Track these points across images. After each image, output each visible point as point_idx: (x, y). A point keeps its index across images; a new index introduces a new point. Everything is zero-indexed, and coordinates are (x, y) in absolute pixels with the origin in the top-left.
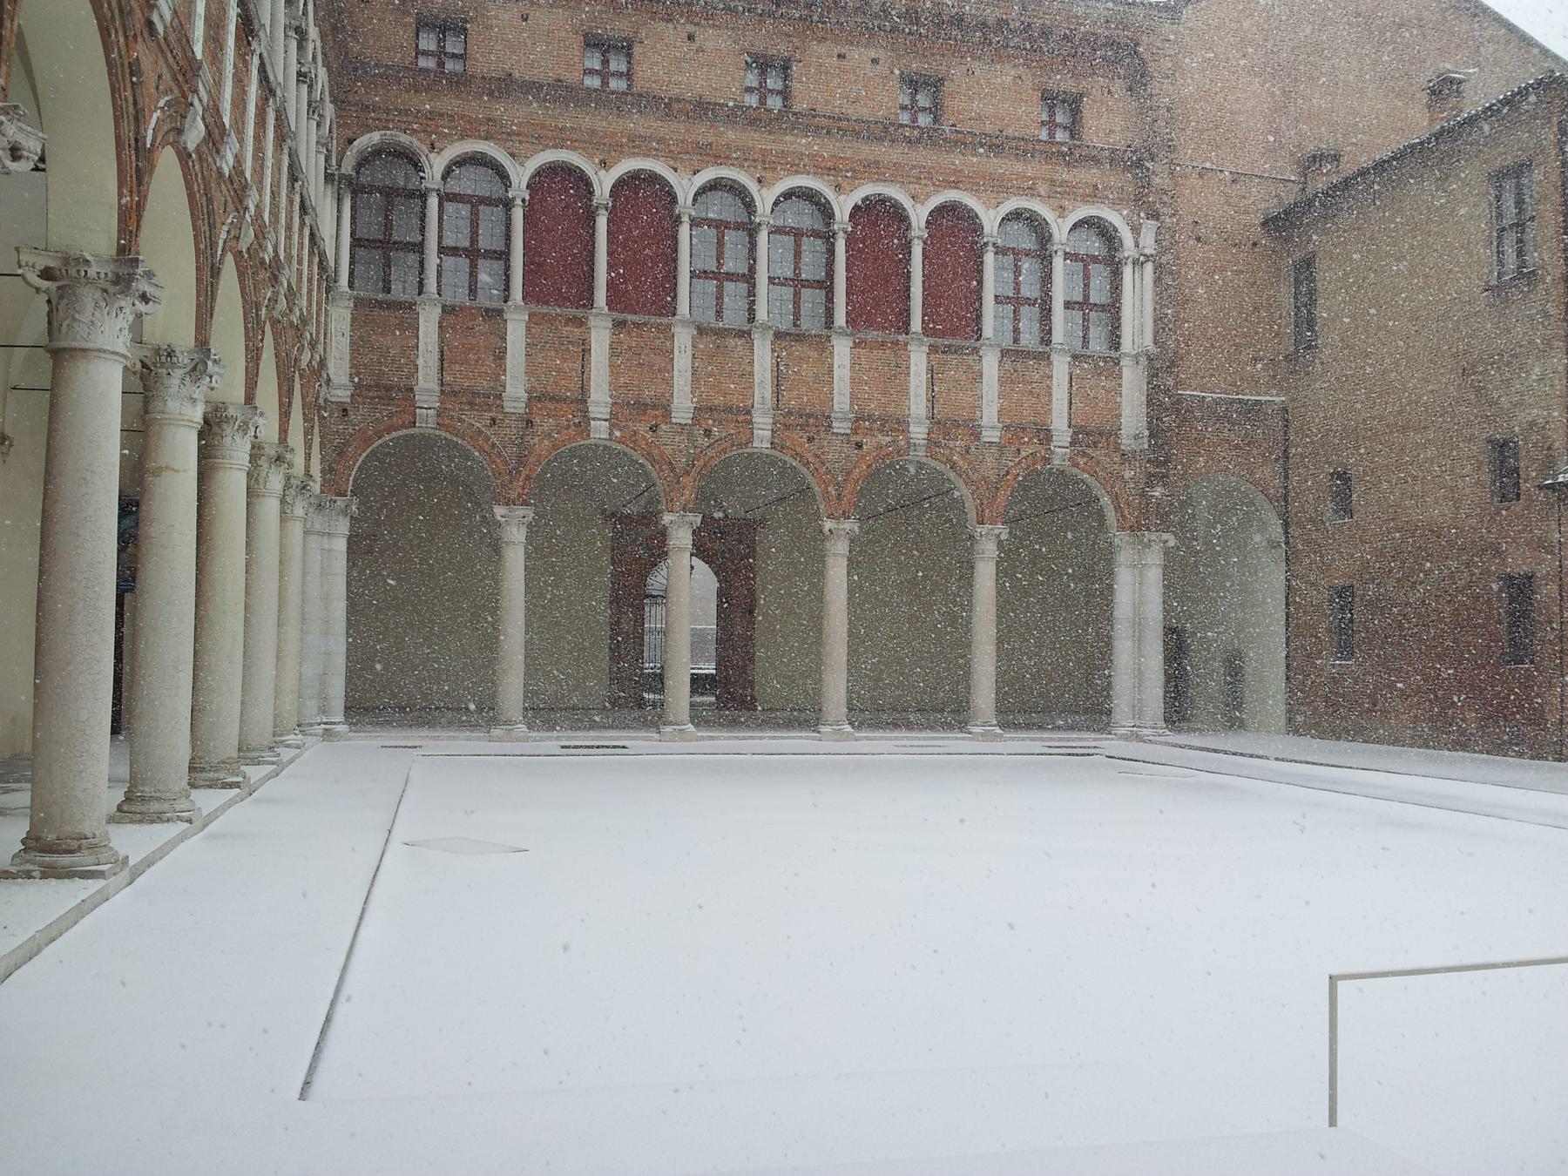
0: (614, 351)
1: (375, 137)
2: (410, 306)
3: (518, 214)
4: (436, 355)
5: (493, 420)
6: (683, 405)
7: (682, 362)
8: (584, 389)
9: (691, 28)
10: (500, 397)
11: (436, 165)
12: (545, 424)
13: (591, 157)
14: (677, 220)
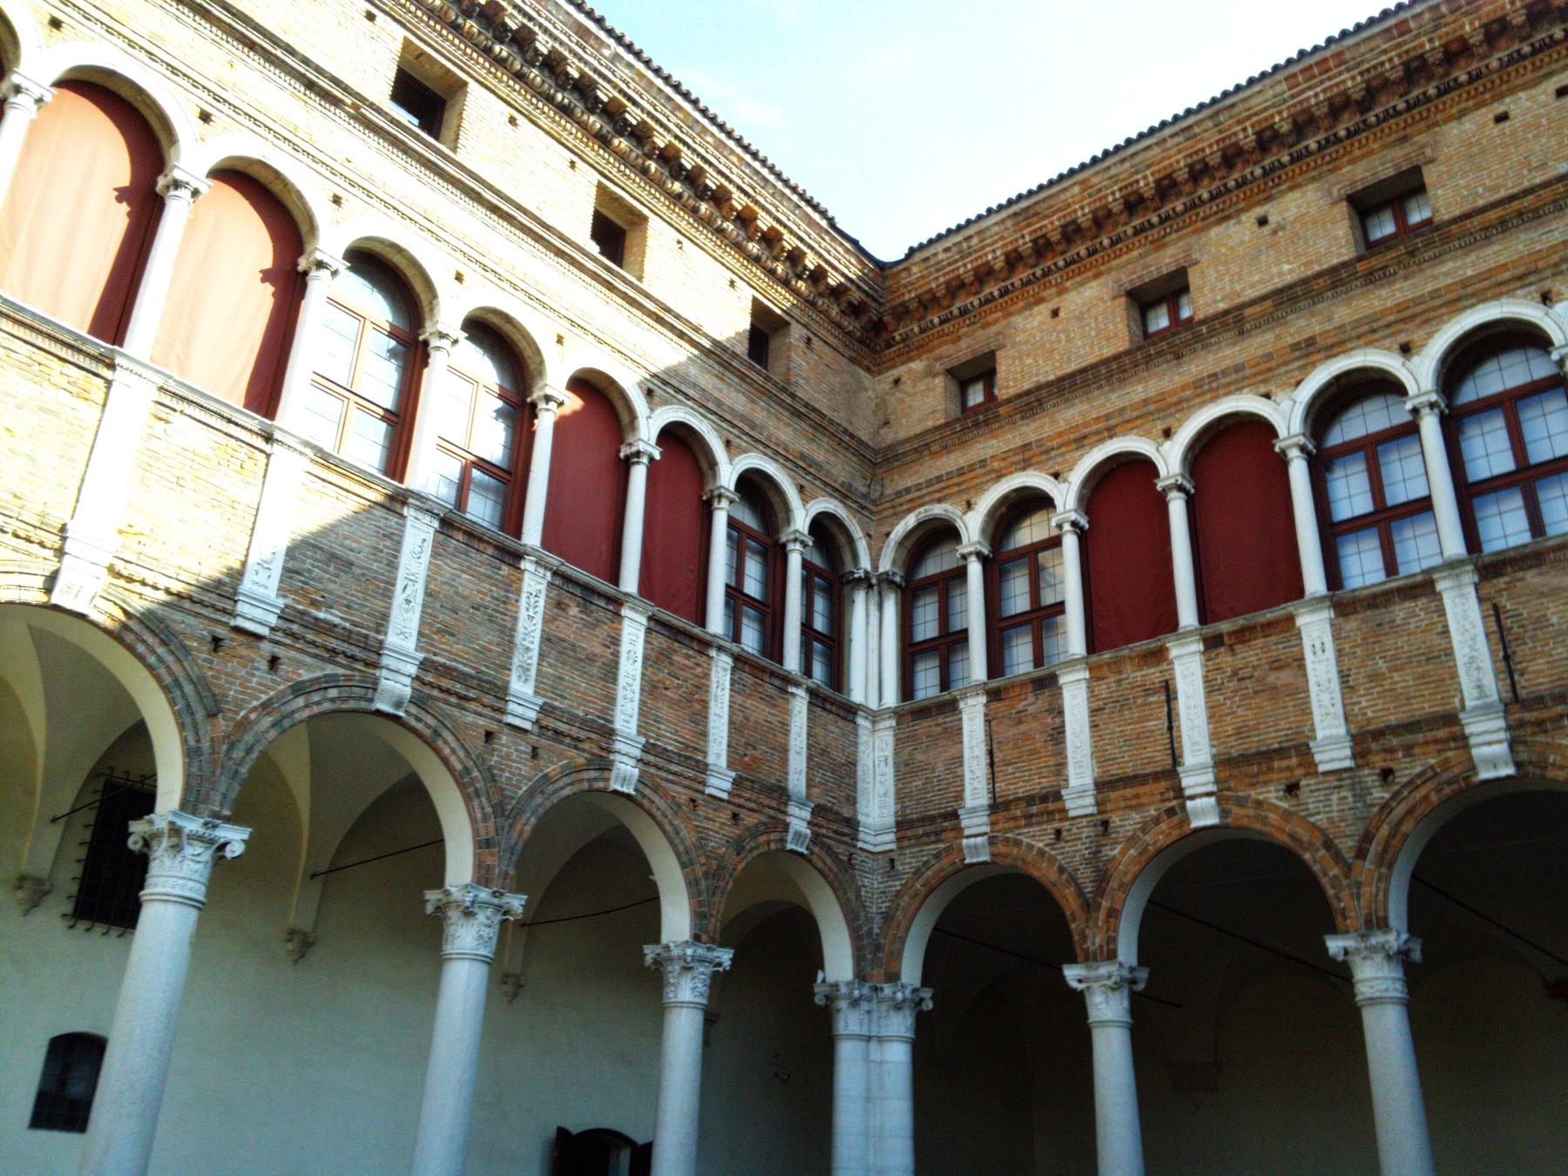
0: (1211, 687)
1: (910, 521)
2: (951, 707)
3: (1070, 543)
4: (984, 760)
5: (1058, 832)
6: (1331, 742)
7: (1321, 669)
8: (1176, 758)
9: (1259, 211)
10: (1058, 797)
11: (972, 527)
12: (1126, 822)
13: (1147, 434)
14: (1282, 462)
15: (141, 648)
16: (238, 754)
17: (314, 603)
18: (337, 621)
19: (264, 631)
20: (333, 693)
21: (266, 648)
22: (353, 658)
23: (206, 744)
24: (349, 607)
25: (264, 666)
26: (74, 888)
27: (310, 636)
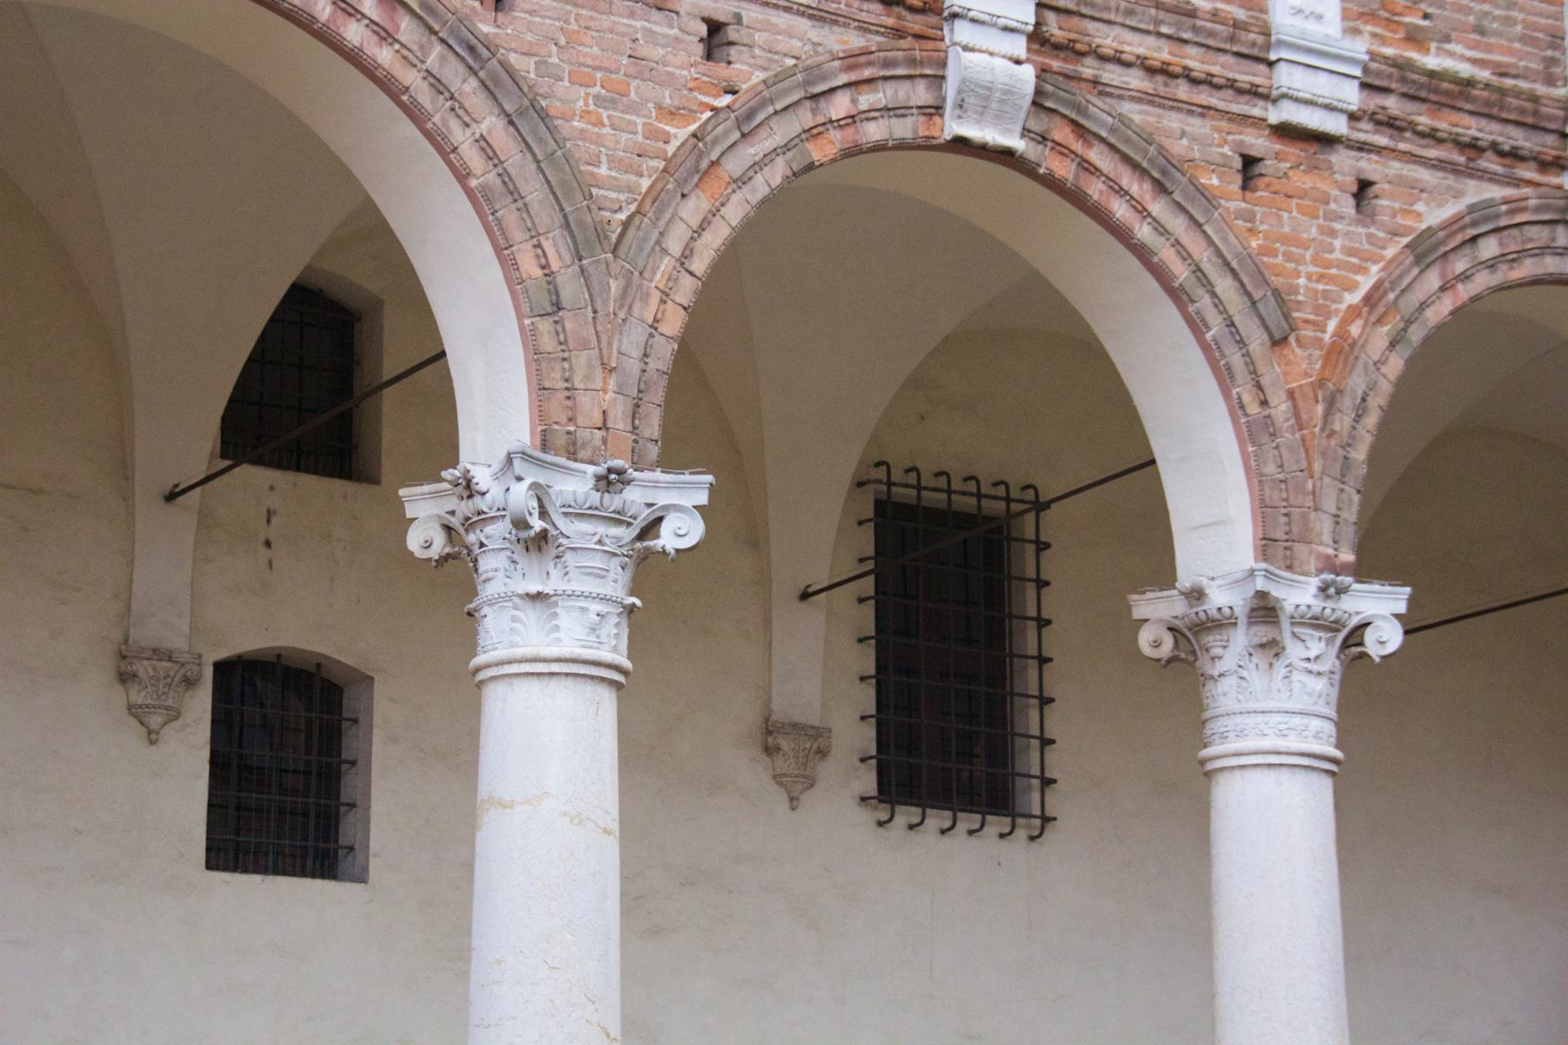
15: (1120, 210)
16: (1342, 423)
17: (1414, 38)
18: (1465, 70)
19: (1335, 125)
20: (1489, 248)
21: (1345, 163)
22: (1514, 155)
23: (1280, 408)
24: (1480, 30)
25: (1347, 206)
26: (867, 738)
27: (1424, 121)
